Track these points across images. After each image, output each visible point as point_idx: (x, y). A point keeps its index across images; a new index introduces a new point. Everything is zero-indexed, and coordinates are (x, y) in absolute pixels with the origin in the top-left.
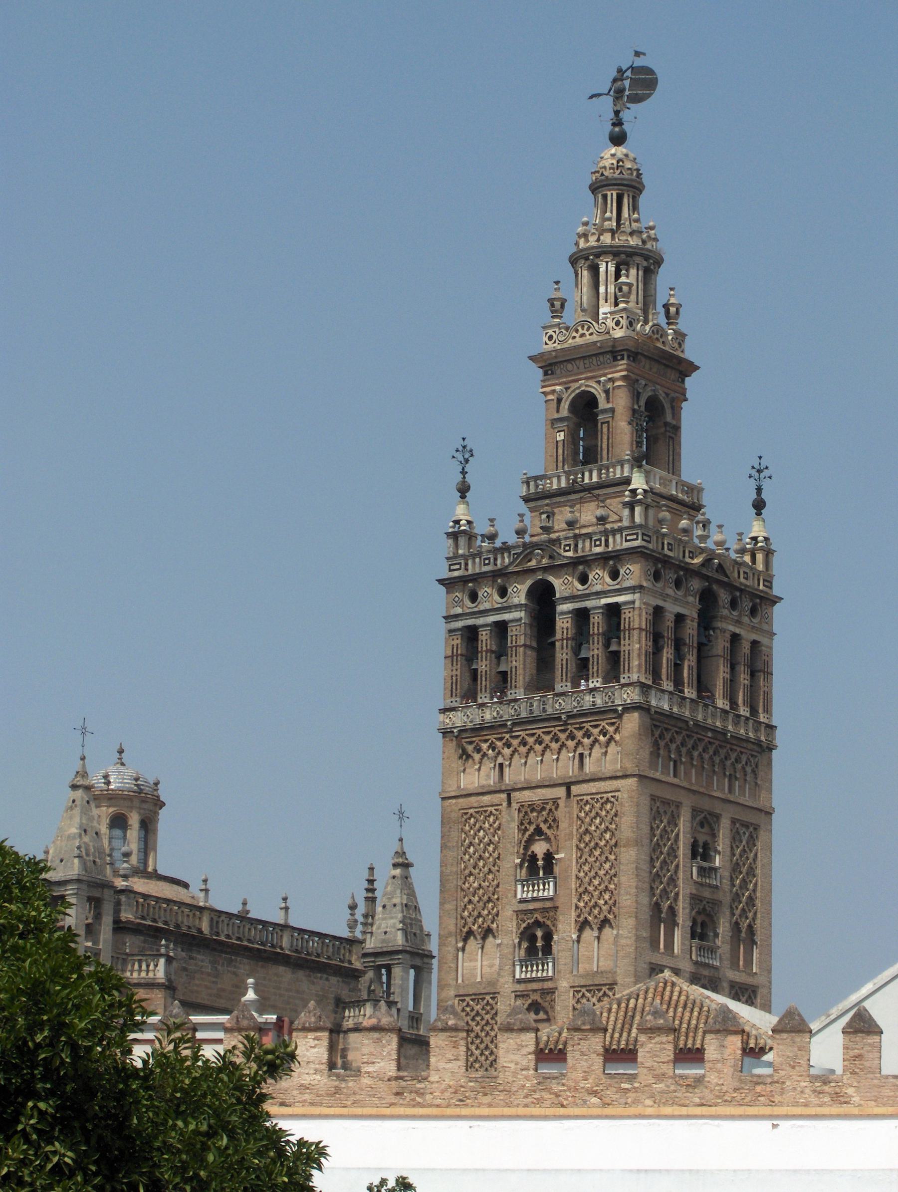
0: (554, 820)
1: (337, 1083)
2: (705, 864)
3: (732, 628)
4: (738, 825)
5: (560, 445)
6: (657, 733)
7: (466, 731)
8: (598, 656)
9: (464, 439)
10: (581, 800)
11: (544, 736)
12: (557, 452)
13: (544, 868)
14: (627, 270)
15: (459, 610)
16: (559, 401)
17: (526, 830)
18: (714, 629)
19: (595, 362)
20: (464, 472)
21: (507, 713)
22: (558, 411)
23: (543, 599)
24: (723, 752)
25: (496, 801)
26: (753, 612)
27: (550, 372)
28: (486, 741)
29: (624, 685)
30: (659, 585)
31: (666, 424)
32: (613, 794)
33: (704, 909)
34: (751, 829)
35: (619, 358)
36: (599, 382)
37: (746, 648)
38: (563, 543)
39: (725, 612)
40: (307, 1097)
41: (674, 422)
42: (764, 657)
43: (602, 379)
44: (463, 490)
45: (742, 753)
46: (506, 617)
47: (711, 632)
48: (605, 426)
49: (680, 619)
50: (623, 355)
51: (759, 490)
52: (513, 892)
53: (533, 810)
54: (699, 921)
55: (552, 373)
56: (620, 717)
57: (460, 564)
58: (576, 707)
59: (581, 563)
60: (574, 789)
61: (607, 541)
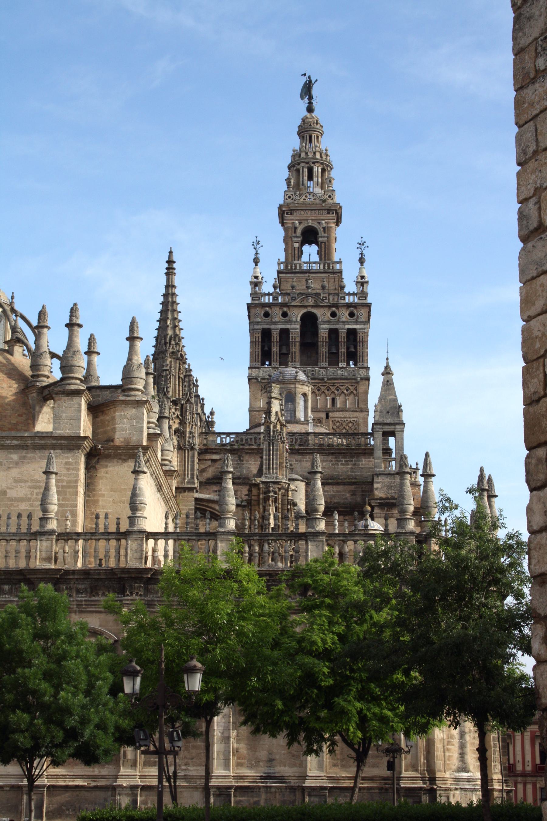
7: (264, 379)
15: (260, 320)
16: (296, 228)
20: (257, 253)
22: (295, 232)
29: (360, 368)
36: (319, 223)
38: (322, 295)
43: (323, 222)
44: (256, 261)
46: (288, 326)
48: (323, 245)
55: (291, 214)
56: (358, 383)
59: (333, 306)
60: (331, 415)
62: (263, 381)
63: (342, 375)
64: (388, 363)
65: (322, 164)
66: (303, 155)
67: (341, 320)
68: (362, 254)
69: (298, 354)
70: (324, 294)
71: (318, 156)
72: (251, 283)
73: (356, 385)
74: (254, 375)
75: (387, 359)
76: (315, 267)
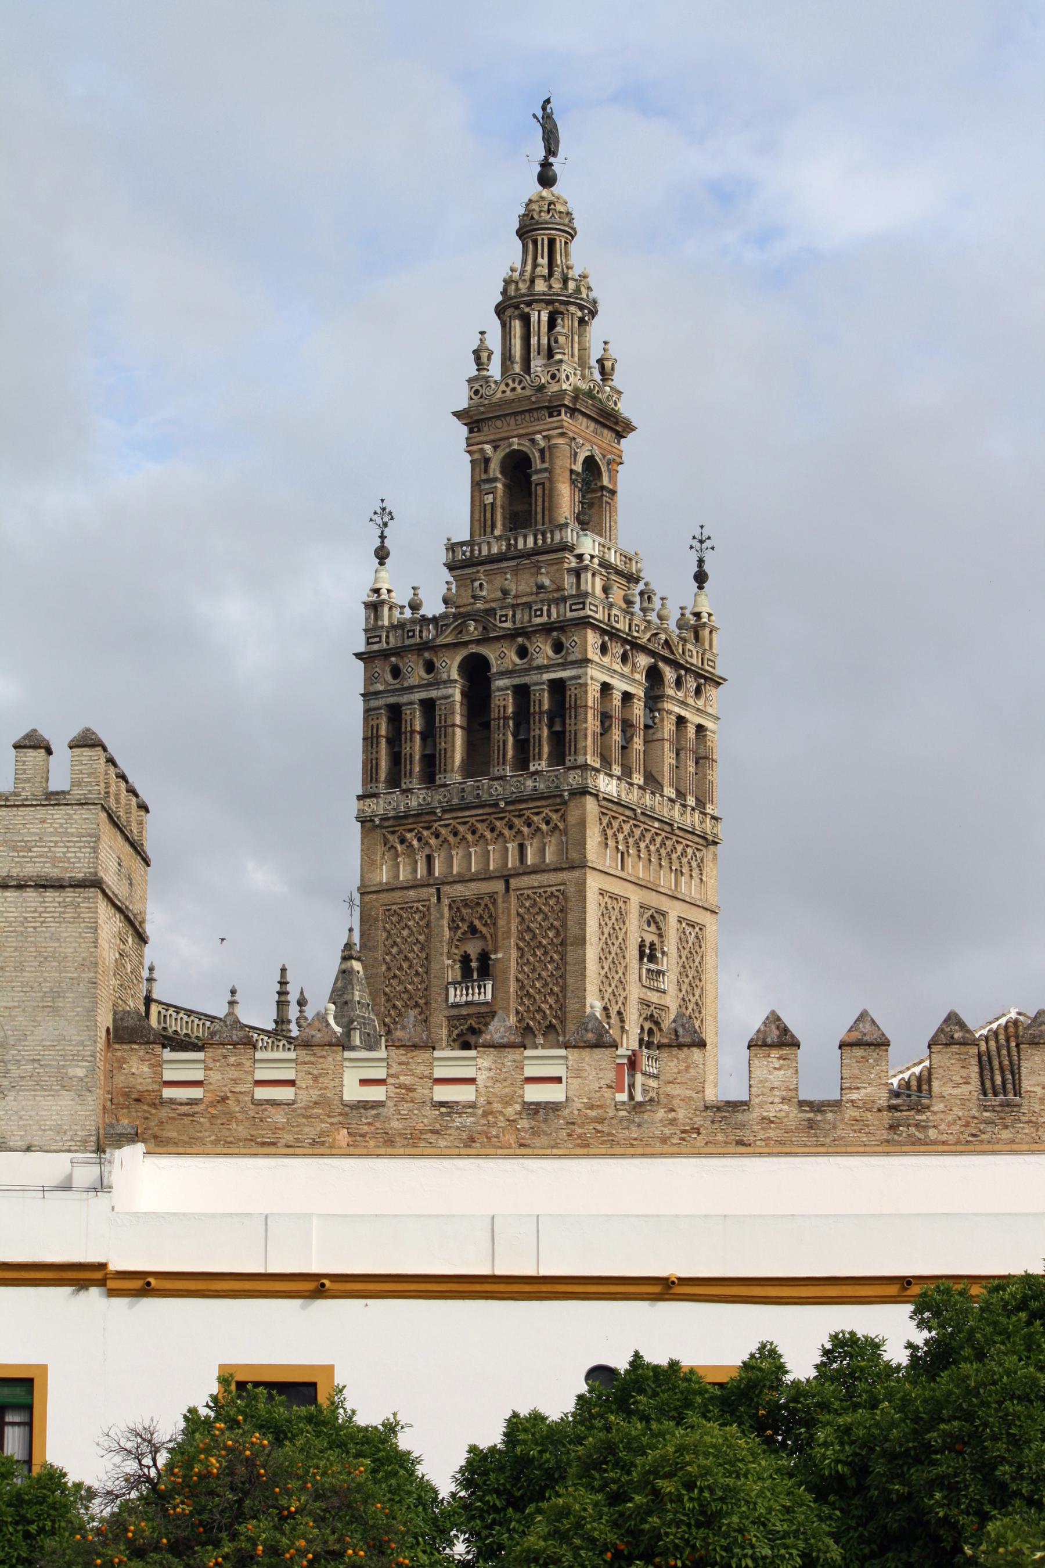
0: (491, 916)
1: (811, 1115)
2: (653, 967)
3: (677, 710)
4: (684, 925)
5: (489, 508)
6: (605, 821)
7: (388, 819)
9: (382, 500)
10: (522, 894)
11: (479, 825)
13: (479, 969)
14: (563, 320)
16: (487, 461)
17: (458, 927)
18: (659, 710)
19: (527, 418)
20: (382, 537)
21: (436, 798)
22: (486, 471)
23: (476, 671)
24: (669, 843)
25: (424, 896)
26: (698, 692)
28: (411, 831)
29: (570, 768)
30: (606, 660)
31: (603, 488)
32: (558, 888)
33: (652, 1016)
34: (697, 929)
35: (555, 414)
37: (691, 730)
38: (499, 613)
39: (670, 692)
40: (771, 1134)
41: (611, 487)
42: (709, 743)
43: (538, 437)
44: (382, 555)
45: (687, 846)
46: (434, 694)
47: (657, 714)
49: (627, 697)
51: (701, 562)
52: (443, 996)
53: (466, 905)
54: (646, 1028)
55: (479, 431)
56: (565, 803)
57: (380, 636)
58: (513, 793)
60: (514, 883)
61: (549, 611)
62: (386, 824)
63: (535, 789)
65: (549, 302)
67: (535, 664)
70: (502, 608)
72: (368, 605)
73: (563, 807)
74: (368, 811)
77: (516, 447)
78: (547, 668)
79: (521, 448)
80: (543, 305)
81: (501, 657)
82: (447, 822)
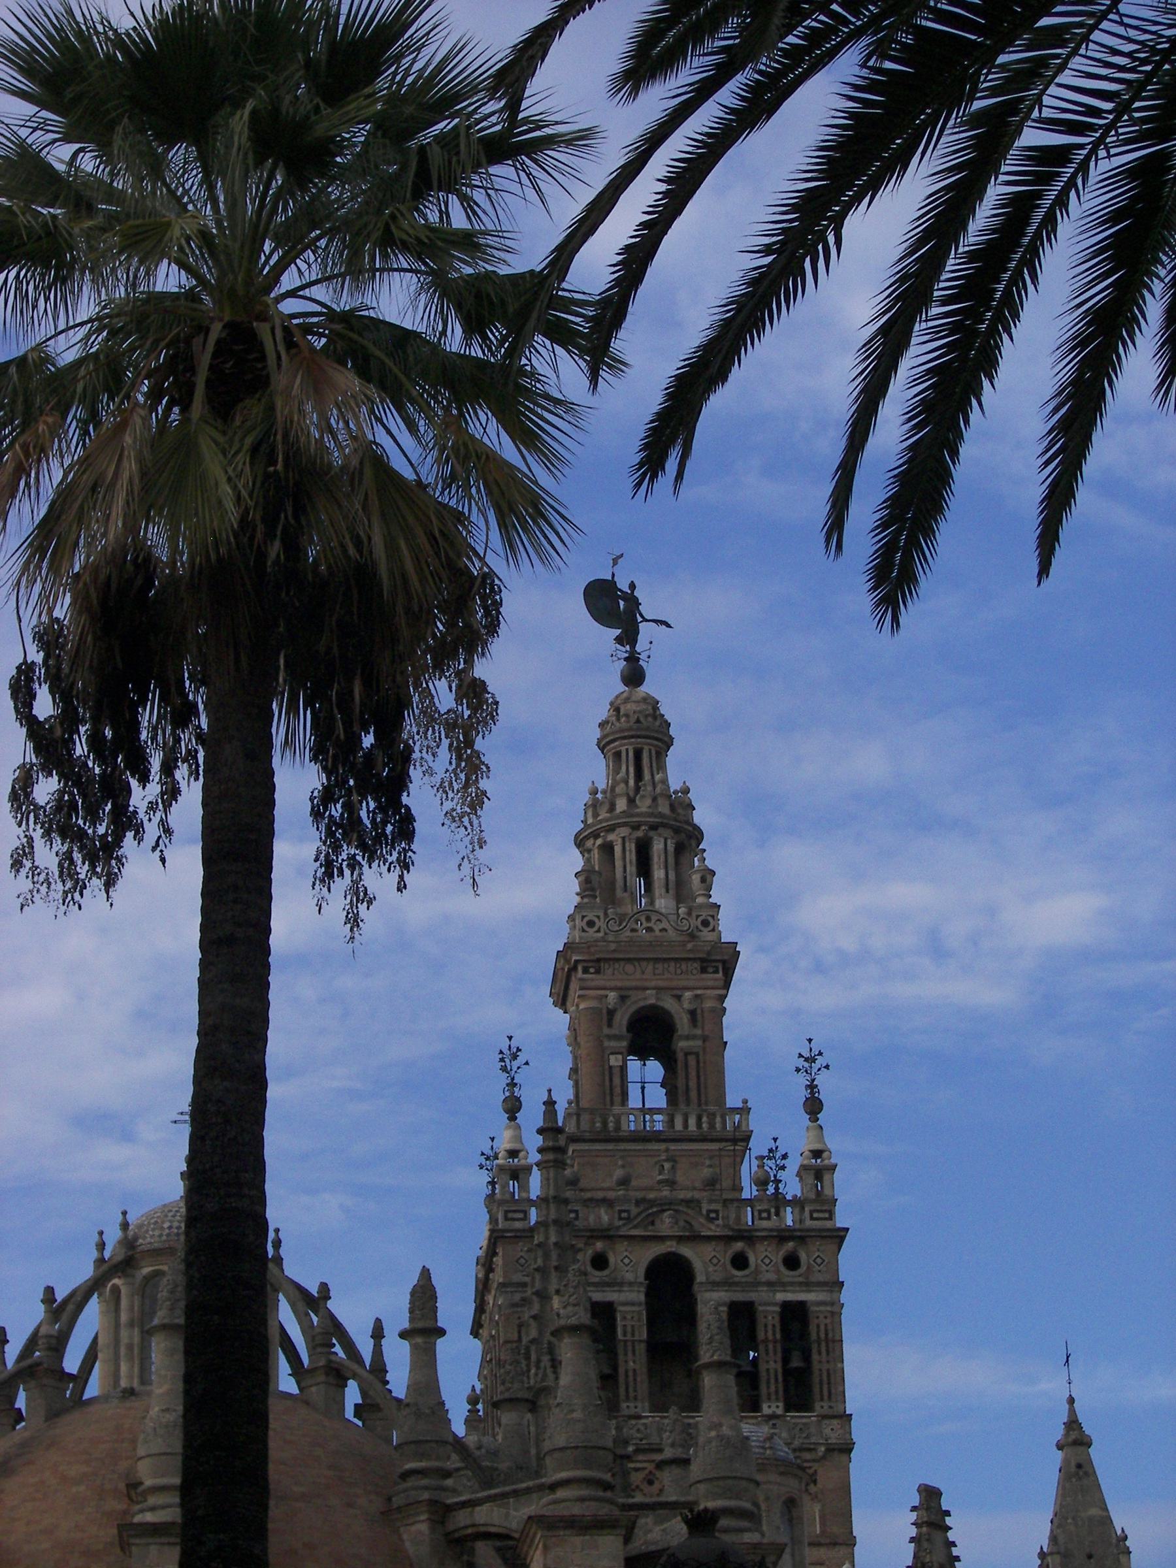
8: (776, 1372)
12: (611, 1080)
16: (611, 1013)
19: (672, 969)
20: (512, 1084)
22: (610, 1025)
27: (592, 970)
29: (825, 1417)
35: (711, 970)
38: (705, 1207)
43: (688, 994)
46: (611, 1296)
50: (717, 968)
55: (598, 972)
64: (1072, 1412)
65: (677, 831)
66: (621, 805)
68: (812, 1087)
69: (643, 1377)
70: (711, 1201)
71: (664, 808)
75: (1071, 1401)
76: (658, 1123)
77: (652, 1001)
78: (783, 1285)
79: (660, 1004)
80: (668, 833)
81: (704, 1261)
82: (639, 1465)
